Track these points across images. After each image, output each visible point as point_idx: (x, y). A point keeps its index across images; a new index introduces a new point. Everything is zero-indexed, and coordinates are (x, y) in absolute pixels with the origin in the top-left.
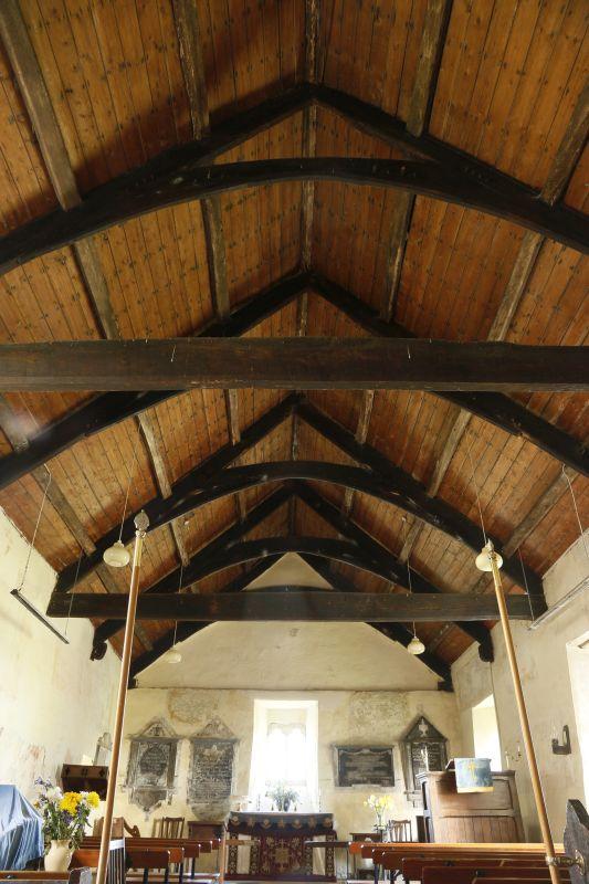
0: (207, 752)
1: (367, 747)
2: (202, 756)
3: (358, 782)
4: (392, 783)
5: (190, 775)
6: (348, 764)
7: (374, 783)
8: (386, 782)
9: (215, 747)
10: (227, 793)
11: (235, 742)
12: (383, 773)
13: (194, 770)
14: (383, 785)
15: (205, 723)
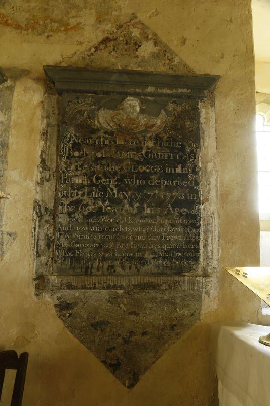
0: (104, 119)
2: (88, 130)
5: (47, 194)
9: (133, 105)
10: (185, 255)
11: (202, 86)
13: (60, 177)
15: (91, 35)
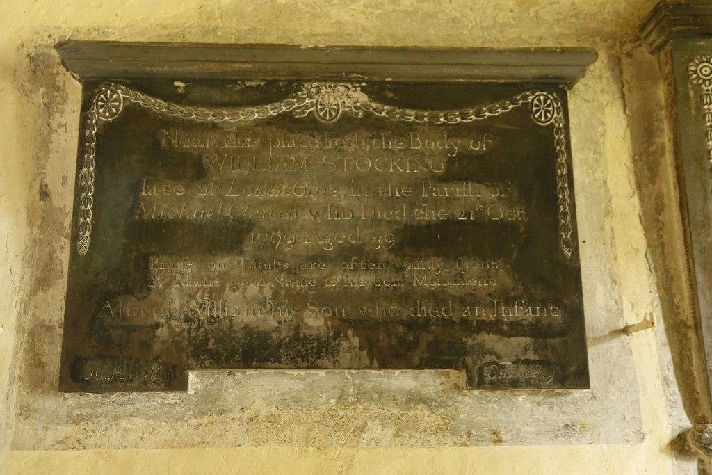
1: (340, 64)
3: (254, 352)
4: (562, 360)
6: (166, 200)
7: (391, 355)
8: (508, 348)
12: (475, 275)
14: (487, 378)
